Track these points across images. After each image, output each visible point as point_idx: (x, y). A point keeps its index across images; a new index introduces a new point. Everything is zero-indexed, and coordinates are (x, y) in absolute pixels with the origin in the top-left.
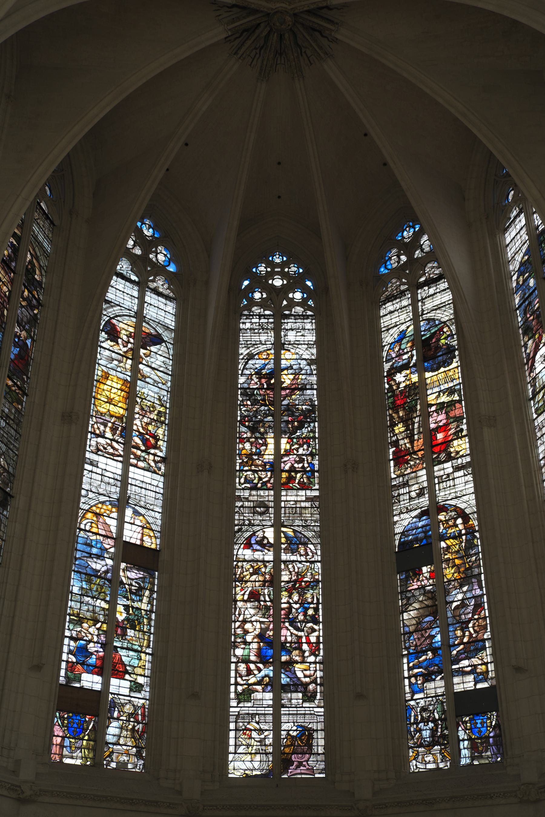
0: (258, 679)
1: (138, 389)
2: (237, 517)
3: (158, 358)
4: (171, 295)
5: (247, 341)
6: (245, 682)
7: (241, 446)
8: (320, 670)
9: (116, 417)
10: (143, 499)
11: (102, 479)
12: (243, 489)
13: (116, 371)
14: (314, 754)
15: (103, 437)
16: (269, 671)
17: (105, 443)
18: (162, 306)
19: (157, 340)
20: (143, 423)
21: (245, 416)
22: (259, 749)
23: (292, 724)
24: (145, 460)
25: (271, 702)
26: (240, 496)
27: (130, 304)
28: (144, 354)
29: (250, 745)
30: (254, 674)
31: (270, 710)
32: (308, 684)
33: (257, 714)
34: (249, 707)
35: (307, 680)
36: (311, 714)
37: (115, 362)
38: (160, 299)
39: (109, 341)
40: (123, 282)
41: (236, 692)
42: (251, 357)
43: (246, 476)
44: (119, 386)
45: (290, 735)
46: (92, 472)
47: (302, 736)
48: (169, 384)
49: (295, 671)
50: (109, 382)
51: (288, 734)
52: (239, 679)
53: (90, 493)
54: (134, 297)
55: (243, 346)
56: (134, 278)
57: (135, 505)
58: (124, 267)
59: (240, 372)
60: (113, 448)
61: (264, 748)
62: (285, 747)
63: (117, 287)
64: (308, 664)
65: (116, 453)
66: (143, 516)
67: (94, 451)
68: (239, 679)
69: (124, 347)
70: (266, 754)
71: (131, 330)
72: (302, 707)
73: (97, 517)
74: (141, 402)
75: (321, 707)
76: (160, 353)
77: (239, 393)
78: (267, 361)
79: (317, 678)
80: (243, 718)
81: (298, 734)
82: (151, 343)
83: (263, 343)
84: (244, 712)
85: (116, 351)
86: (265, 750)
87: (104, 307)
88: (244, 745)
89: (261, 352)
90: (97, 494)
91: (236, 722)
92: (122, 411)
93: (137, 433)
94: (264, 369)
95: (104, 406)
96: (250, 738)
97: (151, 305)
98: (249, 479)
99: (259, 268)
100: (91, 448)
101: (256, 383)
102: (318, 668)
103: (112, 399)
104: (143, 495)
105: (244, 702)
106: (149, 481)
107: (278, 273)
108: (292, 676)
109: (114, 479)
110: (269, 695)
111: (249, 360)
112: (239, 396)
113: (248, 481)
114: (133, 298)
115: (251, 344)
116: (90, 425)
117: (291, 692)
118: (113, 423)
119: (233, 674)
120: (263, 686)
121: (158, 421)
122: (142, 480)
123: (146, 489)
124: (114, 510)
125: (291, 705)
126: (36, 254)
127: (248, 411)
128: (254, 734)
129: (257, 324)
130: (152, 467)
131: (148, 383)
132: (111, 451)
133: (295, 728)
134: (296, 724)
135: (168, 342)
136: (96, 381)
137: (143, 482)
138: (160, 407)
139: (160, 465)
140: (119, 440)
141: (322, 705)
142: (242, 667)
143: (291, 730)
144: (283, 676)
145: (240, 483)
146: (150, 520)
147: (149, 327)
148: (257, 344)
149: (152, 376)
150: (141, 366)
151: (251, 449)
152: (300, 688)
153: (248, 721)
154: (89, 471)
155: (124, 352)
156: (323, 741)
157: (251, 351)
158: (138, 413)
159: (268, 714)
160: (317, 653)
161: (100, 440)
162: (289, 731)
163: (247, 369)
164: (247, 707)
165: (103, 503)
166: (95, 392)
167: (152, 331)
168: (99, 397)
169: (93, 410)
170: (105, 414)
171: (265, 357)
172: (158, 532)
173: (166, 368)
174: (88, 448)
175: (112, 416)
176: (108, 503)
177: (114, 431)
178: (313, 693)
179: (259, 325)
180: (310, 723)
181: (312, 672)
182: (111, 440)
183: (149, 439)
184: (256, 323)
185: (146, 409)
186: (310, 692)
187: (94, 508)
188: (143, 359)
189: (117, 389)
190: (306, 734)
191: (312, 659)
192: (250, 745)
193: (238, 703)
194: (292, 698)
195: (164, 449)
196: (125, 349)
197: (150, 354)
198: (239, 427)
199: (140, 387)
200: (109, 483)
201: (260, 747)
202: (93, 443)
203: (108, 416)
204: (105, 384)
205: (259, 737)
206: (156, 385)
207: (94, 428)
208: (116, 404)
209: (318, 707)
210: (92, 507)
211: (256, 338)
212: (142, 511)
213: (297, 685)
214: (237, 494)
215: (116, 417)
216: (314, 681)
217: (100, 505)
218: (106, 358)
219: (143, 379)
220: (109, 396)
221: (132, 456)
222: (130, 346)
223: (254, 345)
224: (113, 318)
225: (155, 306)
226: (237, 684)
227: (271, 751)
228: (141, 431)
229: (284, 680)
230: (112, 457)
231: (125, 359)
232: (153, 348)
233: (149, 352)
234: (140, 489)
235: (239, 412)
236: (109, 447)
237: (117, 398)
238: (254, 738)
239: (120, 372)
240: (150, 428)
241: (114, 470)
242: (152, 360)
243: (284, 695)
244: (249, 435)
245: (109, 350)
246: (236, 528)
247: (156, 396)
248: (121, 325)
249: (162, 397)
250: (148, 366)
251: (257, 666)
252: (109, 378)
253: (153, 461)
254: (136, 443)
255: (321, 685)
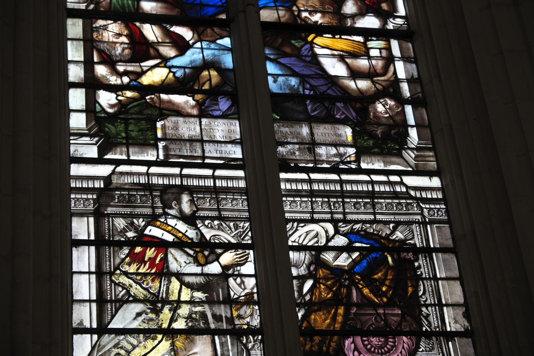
0: (179, 73)
6: (126, 80)
8: (405, 58)
14: (429, 335)
16: (221, 49)
22: (203, 315)
23: (330, 227)
25: (236, 152)
29: (166, 302)
30: (159, 56)
31: (237, 177)
32: (365, 100)
33: (182, 189)
34: (149, 164)
35: (363, 84)
36: (396, 195)
41: (91, 108)
45: (325, 265)
47: (372, 268)
49: (315, 56)
51: (318, 262)
52: (101, 70)
61: (223, 311)
62: (311, 307)
64: (360, 39)
68: (101, 70)
70: (238, 334)
72: (359, 171)
75: (430, 174)
79: (397, 81)
80: (129, 202)
81: (355, 263)
84: (128, 180)
86: (230, 320)
88: (136, 300)
91: (99, 215)
96: (164, 272)
102: (396, 51)
105: (128, 146)
108: (306, 72)
110: (223, 129)
117: (311, 121)
119: (75, 52)
120: (198, 97)
125: (315, 161)
128: (178, 261)
133: (341, 241)
134: (344, 228)
141: (433, 165)
142: (112, 32)
143: (326, 248)
144: (271, 68)
152: (340, 110)
153: (148, 211)
156: (457, 287)
159: (227, 190)
160: (384, 6)
162: (318, 250)
164: (140, 165)
178: (391, 127)
180: (398, 224)
181: (379, 64)
186: (379, 124)
190: (387, 266)
191: (371, 22)
192: (166, 302)
193: (102, 151)
194: (318, 138)
201: (207, 309)
205: (198, 270)
209: (417, 172)
213: (325, 100)
216: (392, 89)
226: (92, 84)
227: (256, 322)
229: (277, 78)
238: (179, 276)
243: (283, 130)
251: (168, 33)
255: (414, 102)
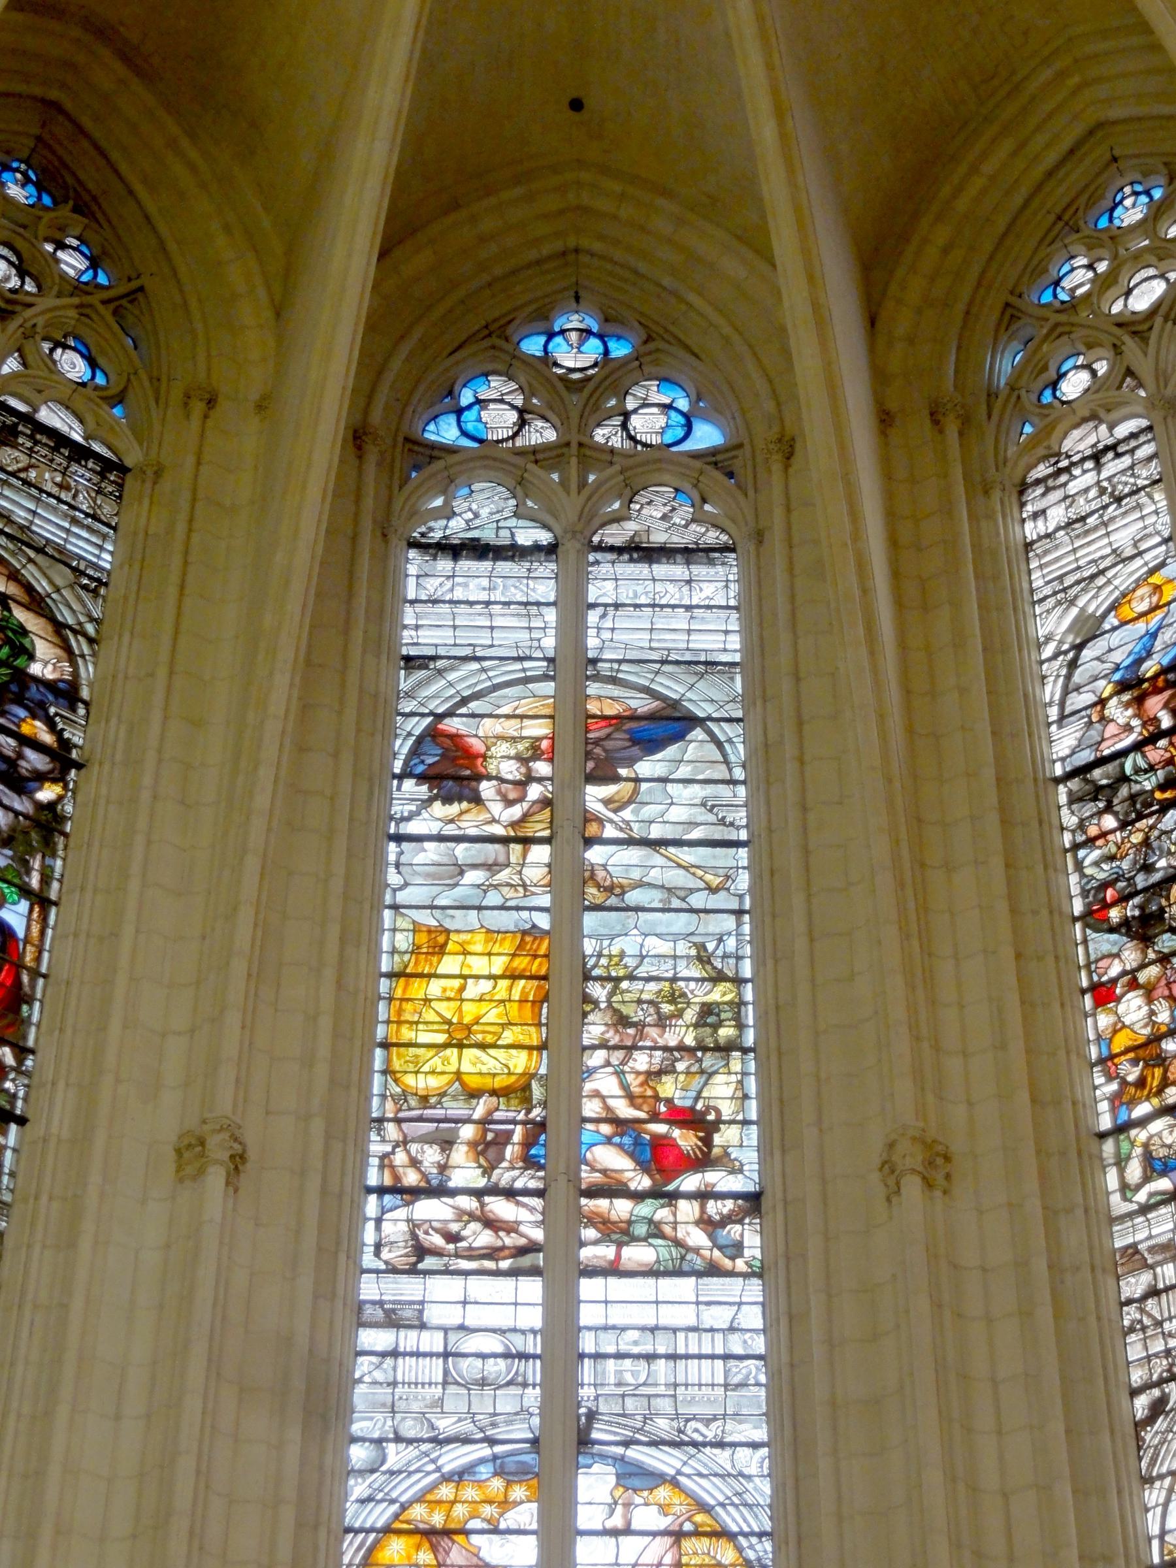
1: (589, 946)
2: (1135, 1352)
3: (683, 793)
4: (713, 537)
5: (1060, 578)
7: (1104, 1020)
9: (494, 1093)
10: (665, 1405)
11: (446, 1372)
12: (1145, 1209)
13: (480, 908)
15: (438, 1190)
17: (448, 1214)
18: (673, 594)
19: (669, 724)
20: (630, 1078)
21: (1105, 885)
24: (656, 1231)
26: (1134, 1246)
27: (525, 635)
28: (607, 802)
37: (474, 877)
38: (661, 569)
39: (437, 805)
40: (486, 565)
42: (1089, 631)
43: (1146, 1146)
44: (498, 965)
46: (395, 1354)
48: (743, 881)
50: (449, 964)
53: (391, 1448)
54: (538, 604)
55: (1051, 602)
56: (528, 535)
57: (626, 1444)
58: (484, 512)
59: (1053, 713)
60: (491, 1223)
63: (459, 594)
65: (509, 1240)
66: (674, 1483)
67: (401, 1263)
69: (509, 803)
71: (538, 729)
73: (434, 1549)
74: (612, 994)
76: (684, 772)
77: (1063, 799)
78: (1155, 619)
82: (635, 750)
83: (1129, 552)
85: (473, 832)
87: (403, 686)
89: (1124, 595)
90: (425, 1447)
92: (520, 1061)
93: (606, 1129)
94: (1149, 654)
95: (436, 1063)
97: (617, 606)
98: (1162, 1152)
99: (1067, 283)
100: (385, 1254)
101: (1128, 728)
103: (468, 1028)
104: (661, 1390)
106: (685, 1316)
107: (1138, 260)
109: (507, 1355)
111: (1079, 648)
112: (1065, 811)
113: (1158, 1165)
114: (534, 610)
115: (1078, 582)
116: (375, 1161)
118: (485, 1122)
121: (705, 1049)
122: (652, 1322)
123: (673, 1357)
124: (518, 1492)
126: (29, 588)
127: (1112, 858)
129: (1093, 493)
130: (696, 1251)
131: (638, 909)
132: (484, 1238)
135: (718, 720)
136: (391, 975)
137: (653, 1330)
138: (707, 986)
139: (734, 1230)
140: (519, 1184)
145: (1124, 1187)
146: (711, 1491)
147: (615, 691)
148: (1102, 572)
149: (654, 875)
150: (595, 855)
151: (1152, 1013)
154: (383, 1355)
155: (514, 825)
157: (1083, 610)
158: (603, 1045)
161: (429, 1209)
163: (1077, 689)
165: (459, 1476)
166: (388, 1022)
167: (634, 704)
168: (407, 1034)
169: (383, 1097)
170: (443, 1094)
171: (1143, 607)
172: (761, 1535)
173: (722, 822)
174: (368, 1259)
175: (473, 1094)
176: (485, 1471)
177: (492, 1153)
179: (1102, 491)
182: (478, 1193)
183: (665, 1137)
184: (1086, 490)
185: (636, 1014)
187: (418, 1512)
188: (600, 821)
189: (490, 977)
195: (749, 1157)
196: (516, 811)
197: (636, 792)
198: (1085, 941)
199: (599, 937)
200: (483, 1383)
202: (395, 1228)
203: (455, 1098)
204: (430, 976)
206: (676, 903)
207: (392, 1167)
208: (489, 1039)
210: (404, 1508)
211: (1097, 548)
212: (664, 1461)
214: (1118, 1244)
215: (494, 1093)
217: (446, 1492)
218: (428, 875)
219: (613, 901)
220: (457, 1017)
221: (590, 1233)
222: (535, 792)
223: (1093, 577)
224: (450, 713)
225: (637, 606)
228: (625, 1110)
230: (489, 1265)
231: (516, 848)
232: (644, 768)
233: (630, 786)
234: (643, 1363)
235: (1074, 879)
236: (474, 1226)
237: (493, 1015)
239: (502, 908)
240: (668, 1088)
241: (501, 1317)
242: (648, 812)
244: (1131, 956)
245: (441, 838)
246: (1142, 1403)
247: (683, 948)
248: (488, 727)
249: (710, 947)
250: (630, 842)
252: (451, 947)
253: (697, 1223)
254: (604, 1172)
